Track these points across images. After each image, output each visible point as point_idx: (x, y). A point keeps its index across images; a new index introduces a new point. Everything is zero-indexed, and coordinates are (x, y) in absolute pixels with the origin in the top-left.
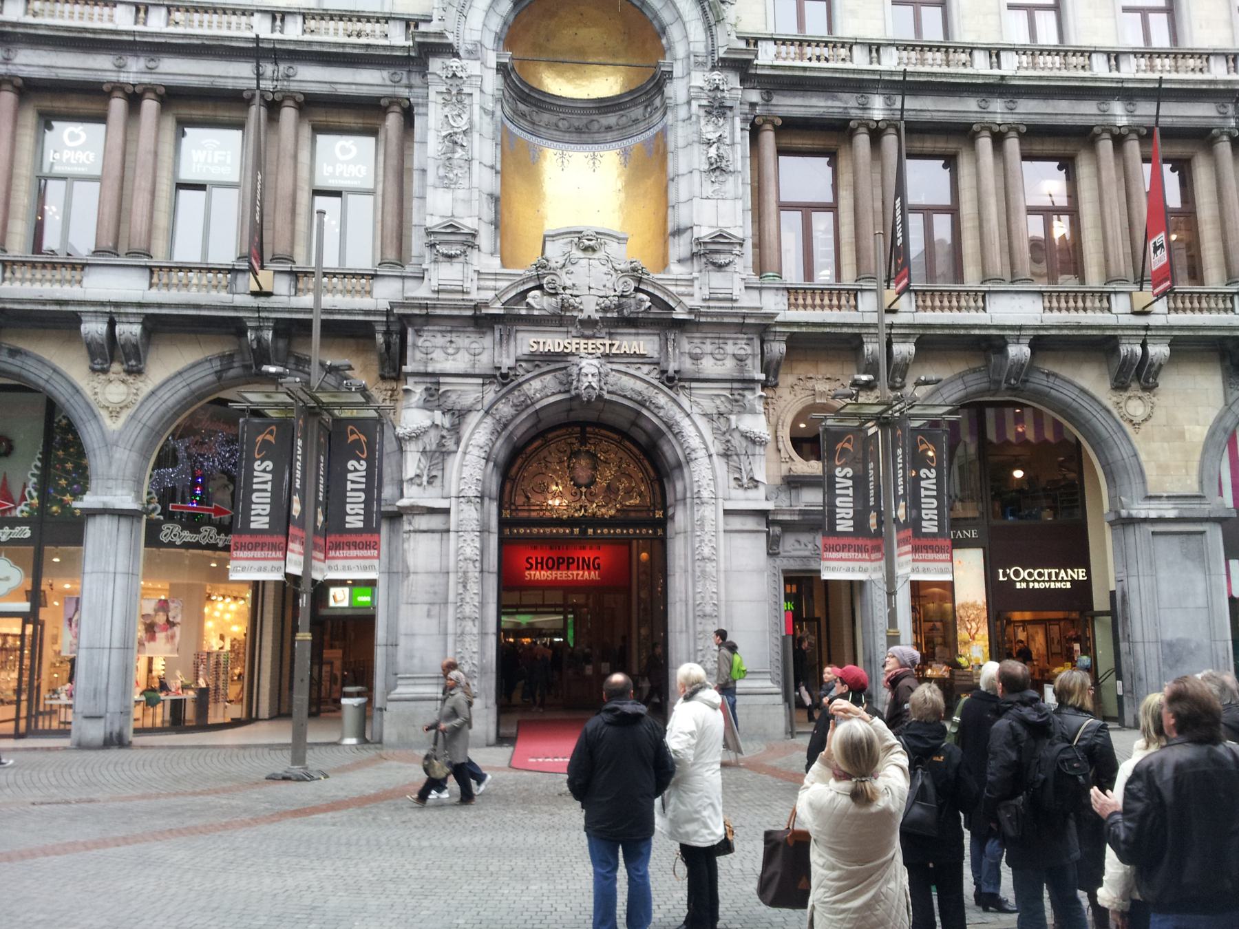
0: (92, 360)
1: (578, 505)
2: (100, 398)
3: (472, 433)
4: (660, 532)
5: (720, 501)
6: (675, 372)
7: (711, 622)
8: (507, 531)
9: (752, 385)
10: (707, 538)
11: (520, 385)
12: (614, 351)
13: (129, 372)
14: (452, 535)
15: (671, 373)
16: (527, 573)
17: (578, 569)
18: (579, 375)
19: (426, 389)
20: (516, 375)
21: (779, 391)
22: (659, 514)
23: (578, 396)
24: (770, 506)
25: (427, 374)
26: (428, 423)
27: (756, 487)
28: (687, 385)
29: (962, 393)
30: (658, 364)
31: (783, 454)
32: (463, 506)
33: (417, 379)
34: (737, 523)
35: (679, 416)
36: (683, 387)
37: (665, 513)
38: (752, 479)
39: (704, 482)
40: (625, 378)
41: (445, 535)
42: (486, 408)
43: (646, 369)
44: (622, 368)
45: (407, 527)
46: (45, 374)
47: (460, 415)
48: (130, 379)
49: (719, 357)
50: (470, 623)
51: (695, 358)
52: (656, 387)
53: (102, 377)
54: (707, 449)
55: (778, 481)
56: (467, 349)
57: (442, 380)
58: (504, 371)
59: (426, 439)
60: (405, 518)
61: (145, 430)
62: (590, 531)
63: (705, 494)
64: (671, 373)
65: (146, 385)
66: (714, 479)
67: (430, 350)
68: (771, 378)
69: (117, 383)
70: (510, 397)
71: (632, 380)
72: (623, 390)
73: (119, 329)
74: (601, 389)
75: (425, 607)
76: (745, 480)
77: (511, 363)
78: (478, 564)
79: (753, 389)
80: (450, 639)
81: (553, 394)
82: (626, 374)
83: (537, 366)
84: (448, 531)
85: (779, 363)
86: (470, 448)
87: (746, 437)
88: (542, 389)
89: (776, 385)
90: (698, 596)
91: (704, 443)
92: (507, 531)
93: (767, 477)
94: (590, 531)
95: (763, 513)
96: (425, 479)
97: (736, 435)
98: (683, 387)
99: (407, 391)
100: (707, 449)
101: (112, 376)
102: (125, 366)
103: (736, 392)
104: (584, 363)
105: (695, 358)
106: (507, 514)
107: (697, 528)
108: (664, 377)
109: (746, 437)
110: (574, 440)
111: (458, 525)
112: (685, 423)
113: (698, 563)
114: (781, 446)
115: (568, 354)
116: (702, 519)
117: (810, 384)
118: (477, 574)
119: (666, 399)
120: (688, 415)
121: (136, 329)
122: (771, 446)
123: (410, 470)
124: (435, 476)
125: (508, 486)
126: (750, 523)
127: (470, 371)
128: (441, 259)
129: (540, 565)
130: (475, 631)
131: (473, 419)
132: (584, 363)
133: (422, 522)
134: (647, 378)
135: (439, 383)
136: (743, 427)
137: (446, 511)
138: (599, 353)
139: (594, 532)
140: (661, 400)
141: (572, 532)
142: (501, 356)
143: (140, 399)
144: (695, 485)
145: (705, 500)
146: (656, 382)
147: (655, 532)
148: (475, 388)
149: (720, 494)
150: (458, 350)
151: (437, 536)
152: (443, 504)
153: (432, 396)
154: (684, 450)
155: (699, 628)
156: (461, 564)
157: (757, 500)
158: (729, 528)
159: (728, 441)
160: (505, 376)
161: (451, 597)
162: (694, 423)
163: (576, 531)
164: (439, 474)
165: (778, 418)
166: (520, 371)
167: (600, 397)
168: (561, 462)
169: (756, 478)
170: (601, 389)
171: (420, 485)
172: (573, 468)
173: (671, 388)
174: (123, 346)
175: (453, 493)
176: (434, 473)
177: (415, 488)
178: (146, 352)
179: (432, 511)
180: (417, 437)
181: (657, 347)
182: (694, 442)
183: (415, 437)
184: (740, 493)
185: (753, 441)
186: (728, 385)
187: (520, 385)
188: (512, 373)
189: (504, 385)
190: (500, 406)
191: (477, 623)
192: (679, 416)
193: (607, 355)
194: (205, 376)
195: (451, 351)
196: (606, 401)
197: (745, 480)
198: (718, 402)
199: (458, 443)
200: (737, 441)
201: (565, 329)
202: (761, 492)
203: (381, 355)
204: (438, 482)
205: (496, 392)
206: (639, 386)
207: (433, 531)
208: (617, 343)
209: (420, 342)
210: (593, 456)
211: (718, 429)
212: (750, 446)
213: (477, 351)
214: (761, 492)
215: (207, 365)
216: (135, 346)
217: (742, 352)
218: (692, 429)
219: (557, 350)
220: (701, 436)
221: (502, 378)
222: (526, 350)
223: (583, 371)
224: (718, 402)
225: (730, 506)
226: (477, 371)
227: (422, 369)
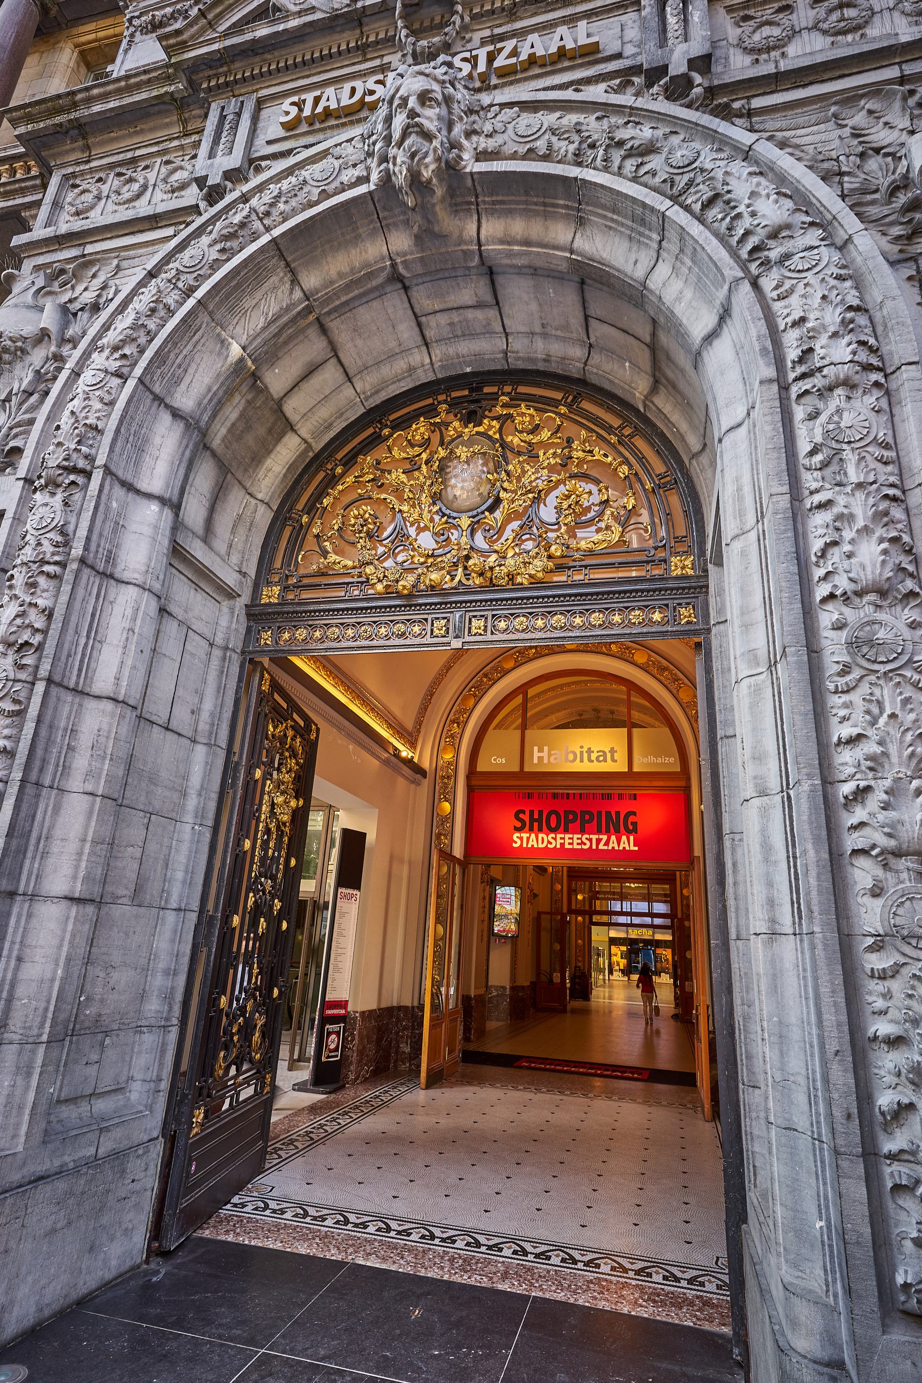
12: (499, 62)
15: (678, 67)
16: (515, 836)
17: (599, 832)
22: (681, 565)
26: (29, 330)
77: (235, 160)
81: (325, 195)
90: (846, 759)
107: (810, 480)
128: (138, 37)
150: (145, 187)
168: (412, 467)
170: (454, 145)
176: (12, 444)
181: (633, 33)
201: (377, 62)
209: (70, 196)
224: (859, 119)
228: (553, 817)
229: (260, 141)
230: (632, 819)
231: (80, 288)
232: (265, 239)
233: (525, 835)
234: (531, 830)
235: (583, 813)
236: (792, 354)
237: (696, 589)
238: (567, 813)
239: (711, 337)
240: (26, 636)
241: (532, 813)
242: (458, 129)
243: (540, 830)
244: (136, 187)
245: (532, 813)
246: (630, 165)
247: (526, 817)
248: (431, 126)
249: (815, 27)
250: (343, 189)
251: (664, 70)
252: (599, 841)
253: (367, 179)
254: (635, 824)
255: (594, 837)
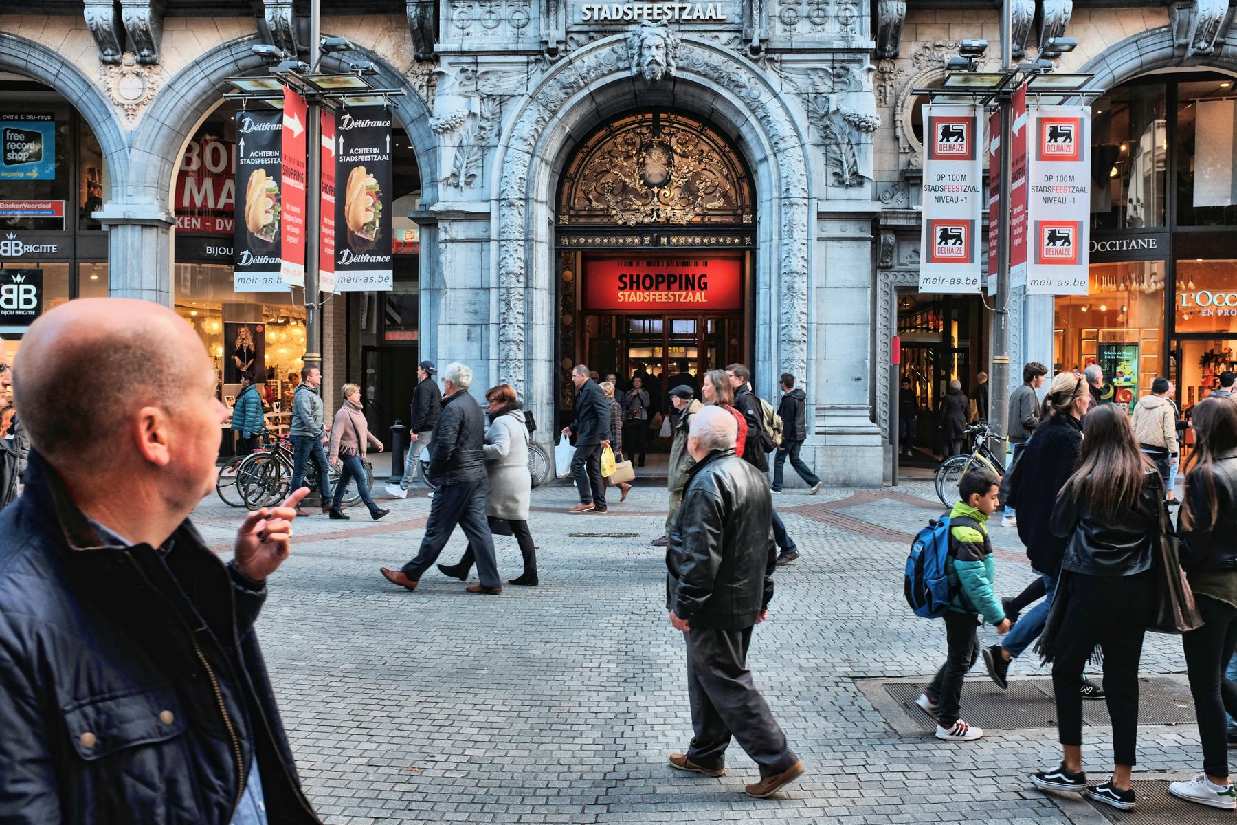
0: (102, 50)
1: (648, 209)
2: (114, 94)
3: (515, 124)
4: (748, 240)
5: (814, 201)
6: (761, 41)
7: (797, 348)
8: (565, 241)
9: (859, 56)
10: (797, 246)
11: (571, 62)
12: (685, 16)
13: (143, 63)
14: (494, 245)
15: (756, 43)
16: (620, 294)
17: (681, 289)
18: (640, 47)
19: (463, 71)
20: (566, 50)
21: (899, 64)
22: (747, 219)
23: (640, 74)
24: (877, 207)
25: (462, 53)
27: (861, 184)
28: (776, 56)
29: (1137, 62)
30: (740, 31)
31: (902, 144)
32: (505, 210)
33: (452, 59)
34: (834, 228)
35: (765, 97)
36: (771, 60)
37: (754, 219)
38: (855, 174)
39: (794, 178)
40: (697, 50)
41: (485, 245)
42: (530, 93)
43: (725, 37)
44: (695, 37)
45: (442, 236)
46: (54, 68)
47: (502, 100)
48: (144, 71)
49: (818, 20)
50: (514, 347)
51: (789, 24)
52: (737, 61)
53: (115, 69)
54: (799, 136)
55: (895, 177)
56: (509, 21)
57: (480, 59)
58: (552, 45)
59: (461, 131)
60: (440, 225)
61: (165, 131)
62: (664, 240)
63: (795, 193)
64: (756, 43)
65: (161, 77)
66: (808, 175)
67: (466, 24)
68: (889, 47)
69: (131, 77)
70: (558, 77)
71: (707, 53)
72: (694, 65)
73: (126, 13)
74: (668, 64)
75: (466, 328)
76: (847, 176)
77: (561, 35)
78: (522, 279)
79: (860, 61)
80: (493, 365)
81: (611, 72)
82: (700, 45)
83: (592, 39)
84: (488, 240)
85: (898, 27)
86: (513, 141)
87: (849, 122)
88: (595, 62)
89: (895, 56)
90: (784, 317)
91: (796, 129)
92: (565, 241)
93: (878, 172)
94: (664, 240)
95: (872, 218)
96: (462, 179)
97: (837, 119)
98: (771, 60)
99: (440, 74)
100: (799, 136)
101: (125, 69)
102: (138, 57)
103: (837, 65)
104: (646, 32)
105: (789, 24)
106: (565, 220)
107: (784, 235)
108: (747, 48)
109: (849, 122)
110: (644, 130)
111: (500, 234)
112: (773, 107)
113: (785, 278)
114: (899, 133)
115: (629, 22)
116: (791, 225)
117: (938, 53)
118: (522, 291)
119: (749, 75)
120: (776, 96)
121: (145, 13)
122: (883, 133)
123: (446, 167)
124: (474, 176)
125: (567, 186)
126: (851, 229)
127: (512, 47)
129: (636, 284)
130: (520, 356)
131: (514, 107)
132: (646, 32)
133: (459, 230)
134: (726, 49)
135: (477, 63)
136: (845, 109)
137: (486, 217)
138: (665, 19)
139: (669, 241)
140: (744, 76)
141: (642, 242)
142: (548, 27)
143: (156, 93)
144: (784, 181)
145: (793, 200)
146: (735, 54)
147: (742, 242)
148: (519, 67)
149: (814, 195)
150: (499, 21)
151: (477, 246)
152: (481, 208)
153: (469, 79)
154: (770, 139)
155: (784, 355)
156: (503, 278)
157: (861, 198)
158: (824, 235)
159: (827, 127)
160: (553, 52)
161: (493, 318)
162: (783, 105)
163: (647, 240)
164: (478, 172)
165: (897, 98)
166: (572, 45)
167: (667, 76)
169: (861, 173)
170: (668, 64)
171: (457, 186)
172: (643, 164)
173: (756, 61)
174: (133, 33)
175: (494, 196)
177: (451, 189)
178: (160, 39)
179: (469, 216)
180: (452, 128)
181: (738, 10)
182: (782, 127)
183: (449, 129)
184: (840, 192)
185: (860, 126)
186: (829, 56)
187: (571, 62)
188: (562, 47)
189: (553, 63)
190: (546, 89)
191: (522, 347)
192: (765, 97)
193: (677, 22)
194: (221, 66)
195: (491, 23)
196: (675, 79)
197: (847, 176)
198: (816, 79)
199: (499, 135)
200: (837, 125)
202: (867, 190)
203: (413, 33)
204: (477, 182)
205: (543, 72)
206: (716, 59)
207: (471, 241)
208: (689, 6)
209: (455, 14)
210: (668, 149)
211: (815, 112)
212: (855, 132)
213: (522, 22)
214: (867, 190)
215: (227, 53)
216: (146, 33)
217: (848, 13)
218: (781, 111)
219: (615, 17)
220: (793, 122)
221: (546, 53)
222: (578, 18)
223: (646, 42)
225: (825, 207)
226: (521, 47)
227: (454, 47)
228: (648, 280)
229: (570, 21)
230: (703, 280)
231: (480, 83)
232: (585, 92)
233: (627, 294)
234: (631, 289)
235: (669, 276)
236: (784, 189)
237: (752, 230)
238: (657, 276)
239: (761, 161)
240: (518, 271)
241: (631, 276)
242: (670, 58)
243: (638, 289)
244: (494, 17)
245: (631, 276)
246: (737, 90)
247: (627, 280)
248: (659, 59)
249: (808, 17)
250: (618, 70)
251: (750, 41)
252: (680, 296)
253: (629, 68)
254: (705, 284)
255: (677, 294)
